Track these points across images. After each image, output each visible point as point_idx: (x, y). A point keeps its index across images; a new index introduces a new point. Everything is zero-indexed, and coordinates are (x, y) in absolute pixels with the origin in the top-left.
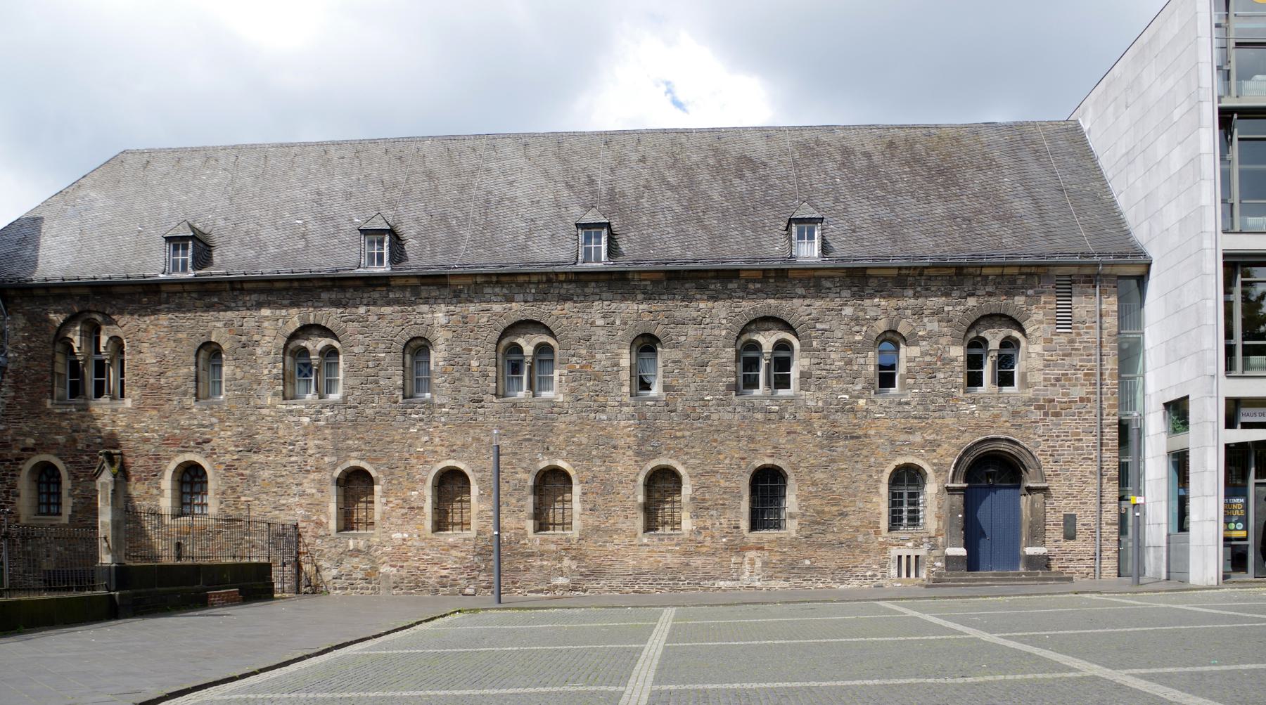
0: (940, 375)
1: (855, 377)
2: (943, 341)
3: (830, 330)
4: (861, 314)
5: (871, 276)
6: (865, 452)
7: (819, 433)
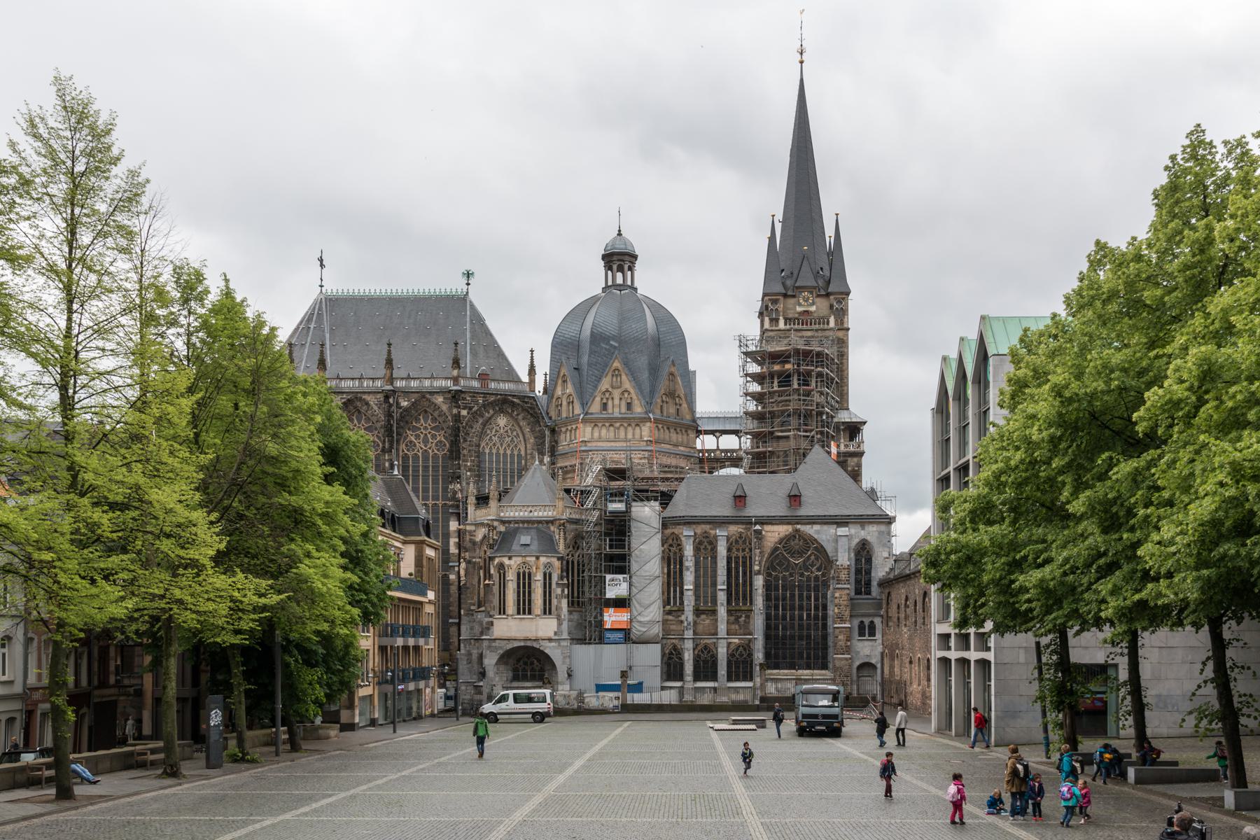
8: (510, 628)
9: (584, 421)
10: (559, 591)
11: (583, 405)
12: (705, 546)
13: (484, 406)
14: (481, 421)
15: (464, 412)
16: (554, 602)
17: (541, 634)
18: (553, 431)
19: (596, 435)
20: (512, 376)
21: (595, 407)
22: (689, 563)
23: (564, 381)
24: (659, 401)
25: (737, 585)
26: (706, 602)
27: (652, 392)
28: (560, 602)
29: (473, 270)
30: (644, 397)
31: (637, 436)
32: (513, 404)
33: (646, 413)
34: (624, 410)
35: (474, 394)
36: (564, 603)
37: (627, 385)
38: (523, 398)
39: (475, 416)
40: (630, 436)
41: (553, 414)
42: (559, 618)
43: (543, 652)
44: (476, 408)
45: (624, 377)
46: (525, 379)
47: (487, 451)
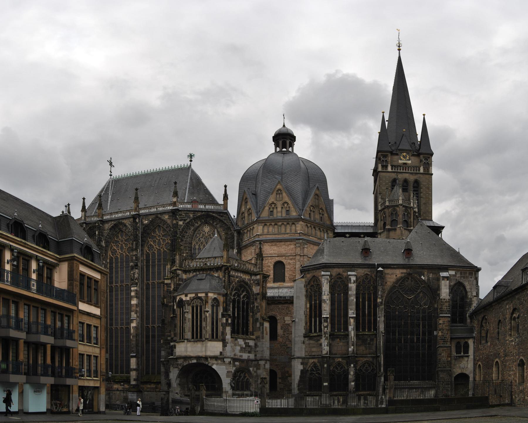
8: (185, 349)
9: (258, 222)
10: (224, 320)
11: (257, 213)
12: (339, 287)
13: (194, 219)
14: (192, 228)
16: (220, 328)
17: (209, 353)
18: (239, 232)
19: (266, 231)
21: (265, 214)
22: (326, 296)
23: (246, 202)
24: (308, 209)
25: (364, 312)
26: (339, 330)
27: (304, 204)
28: (224, 329)
31: (293, 231)
32: (214, 218)
33: (299, 215)
34: (284, 215)
35: (188, 211)
36: (228, 330)
37: (286, 199)
38: (219, 213)
39: (188, 225)
40: (288, 231)
41: (240, 224)
42: (224, 341)
43: (211, 368)
44: (188, 220)
45: (284, 194)
46: (221, 201)
47: (197, 247)
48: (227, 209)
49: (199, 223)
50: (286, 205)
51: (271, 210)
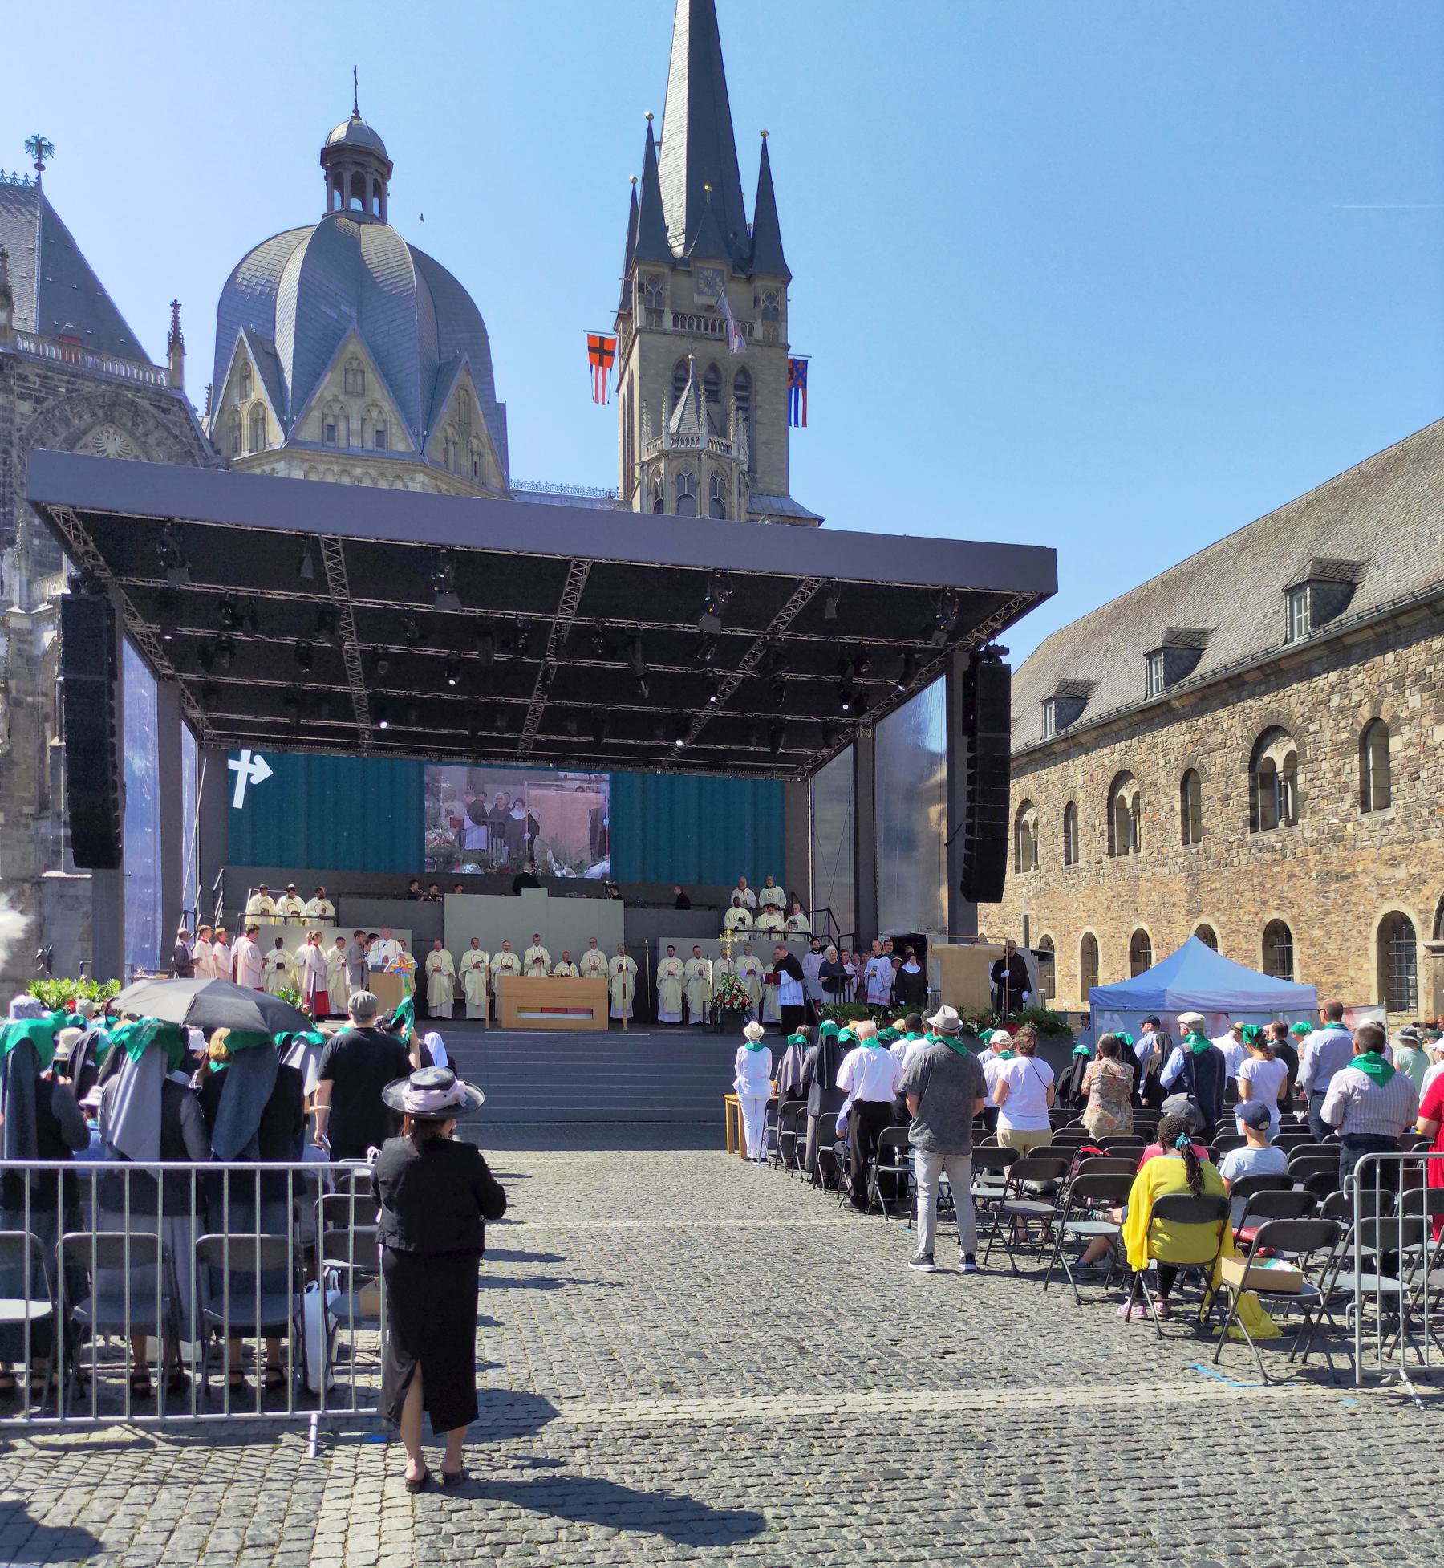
0: (1423, 774)
1: (1344, 788)
2: (1427, 720)
3: (1321, 732)
4: (1346, 701)
5: (1352, 646)
6: (1353, 898)
7: (1314, 875)
11: (285, 426)
15: (25, 407)
20: (132, 350)
29: (50, 138)
30: (410, 423)
37: (378, 392)
45: (372, 378)
46: (158, 355)
48: (181, 389)
49: (87, 417)
50: (375, 414)
51: (330, 421)
